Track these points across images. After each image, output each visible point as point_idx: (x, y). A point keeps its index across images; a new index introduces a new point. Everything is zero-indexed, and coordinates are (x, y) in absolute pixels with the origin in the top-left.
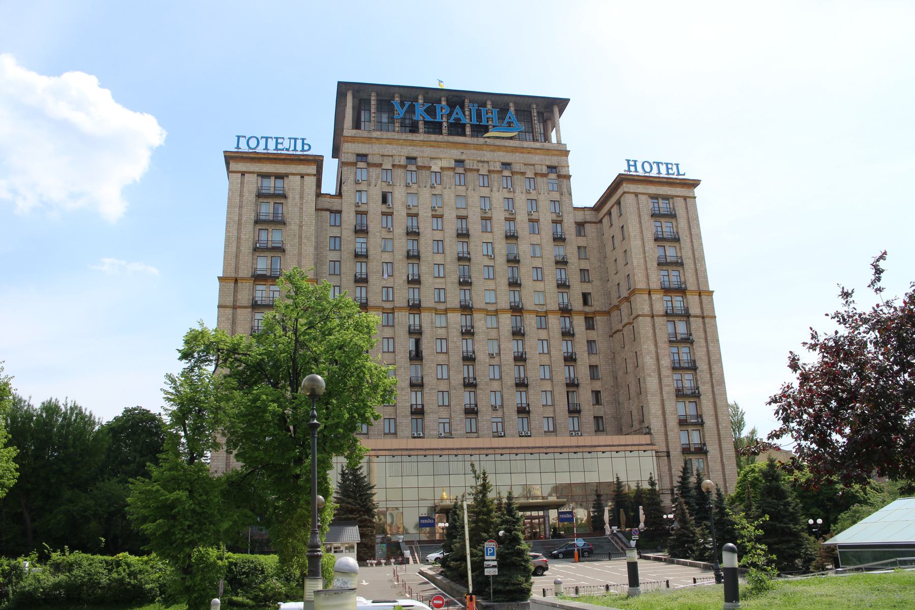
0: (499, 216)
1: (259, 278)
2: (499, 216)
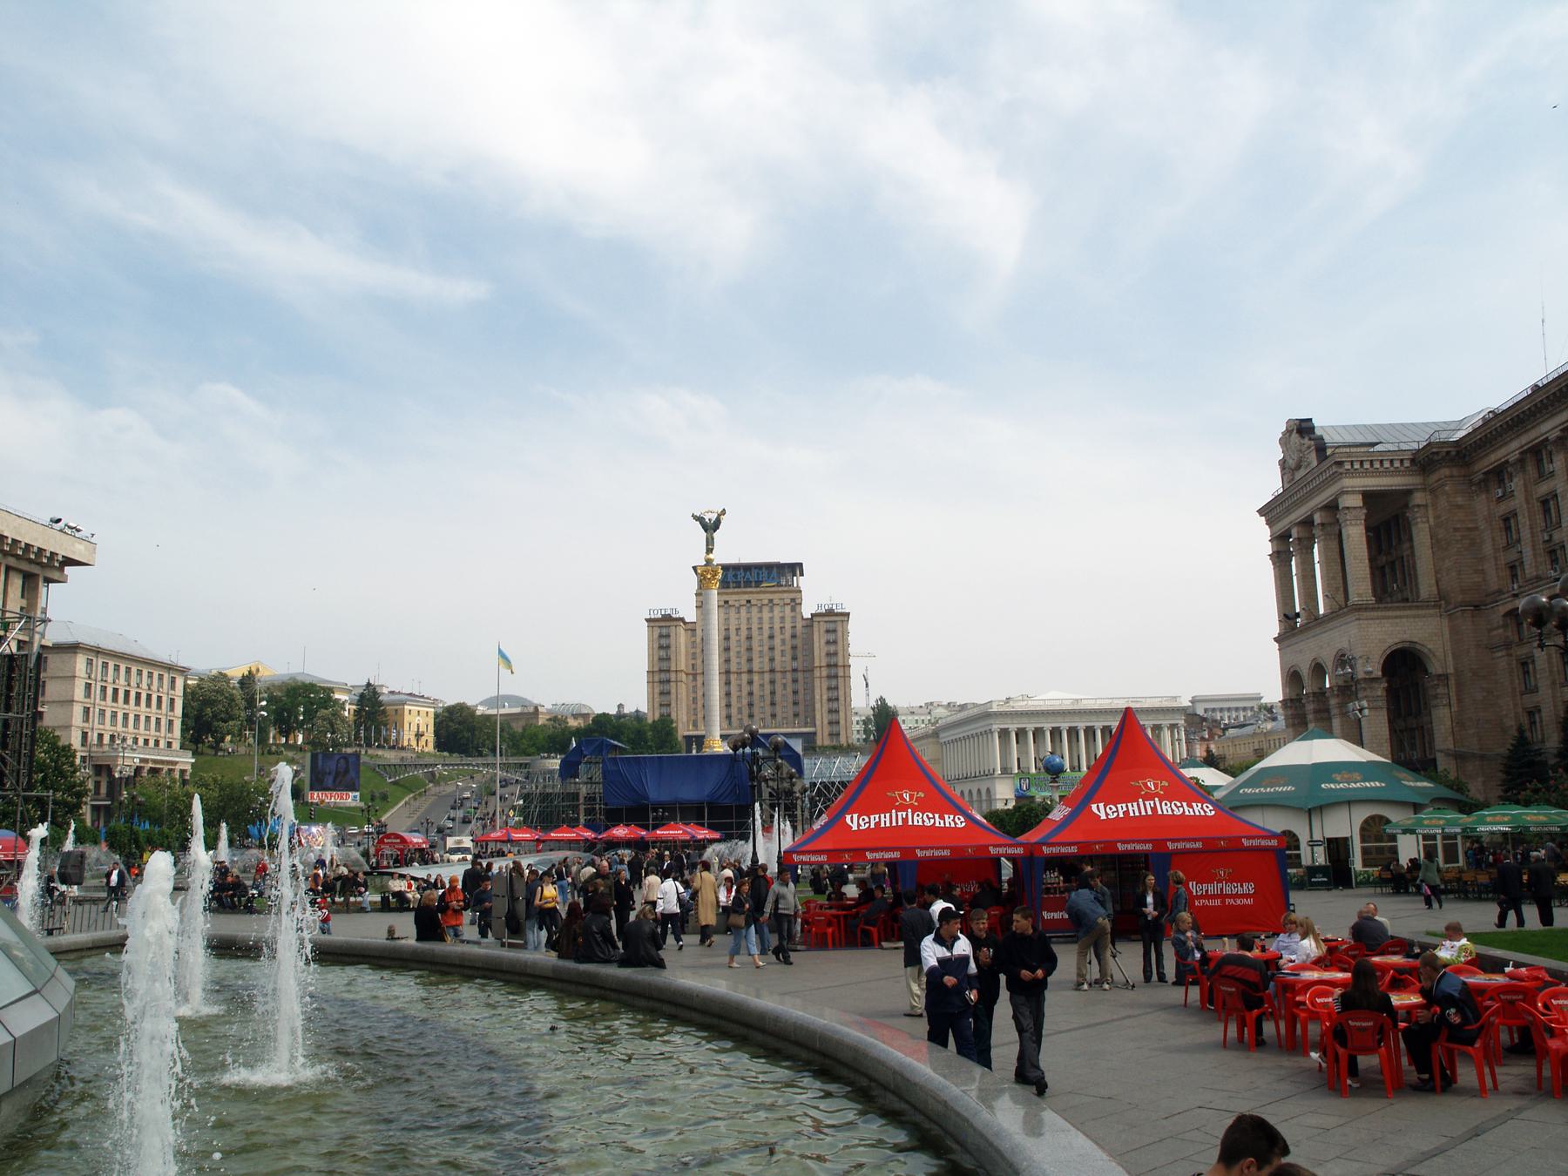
0: (766, 626)
1: (661, 671)
2: (766, 626)
